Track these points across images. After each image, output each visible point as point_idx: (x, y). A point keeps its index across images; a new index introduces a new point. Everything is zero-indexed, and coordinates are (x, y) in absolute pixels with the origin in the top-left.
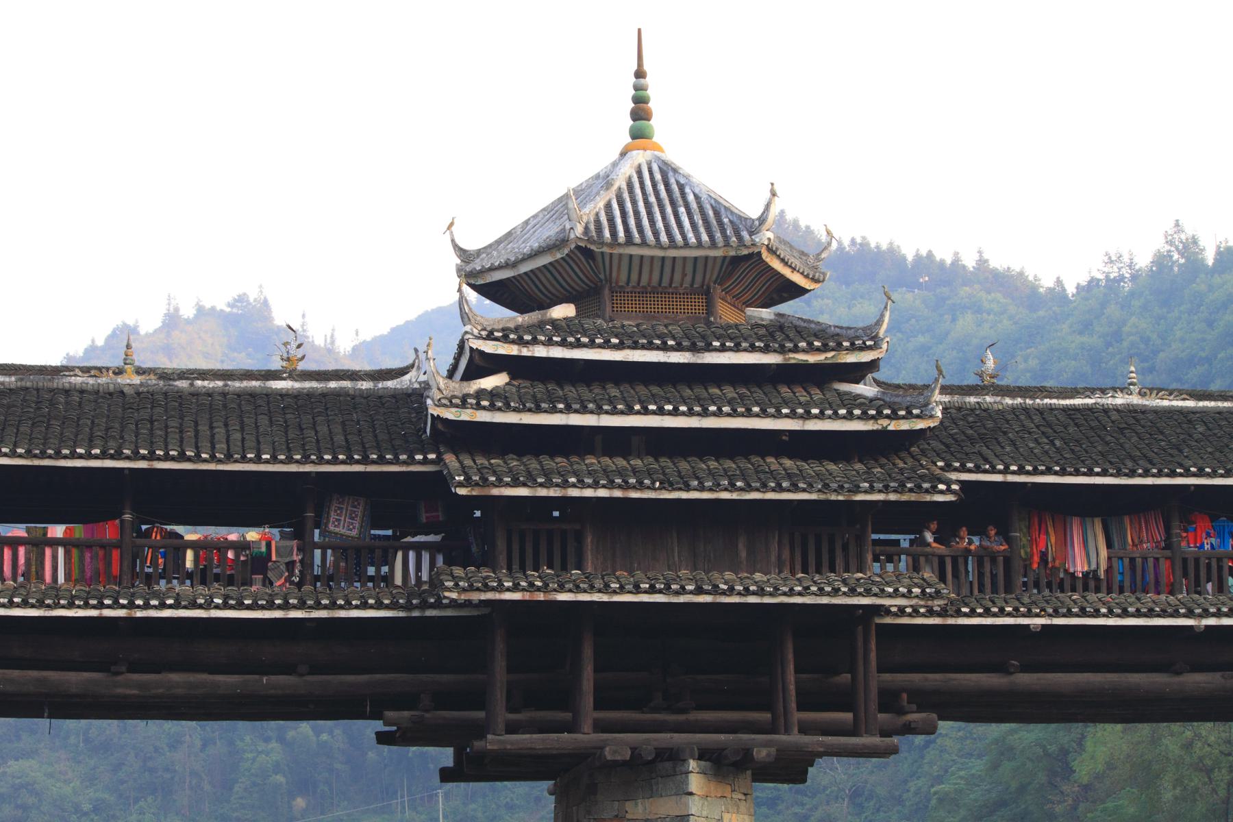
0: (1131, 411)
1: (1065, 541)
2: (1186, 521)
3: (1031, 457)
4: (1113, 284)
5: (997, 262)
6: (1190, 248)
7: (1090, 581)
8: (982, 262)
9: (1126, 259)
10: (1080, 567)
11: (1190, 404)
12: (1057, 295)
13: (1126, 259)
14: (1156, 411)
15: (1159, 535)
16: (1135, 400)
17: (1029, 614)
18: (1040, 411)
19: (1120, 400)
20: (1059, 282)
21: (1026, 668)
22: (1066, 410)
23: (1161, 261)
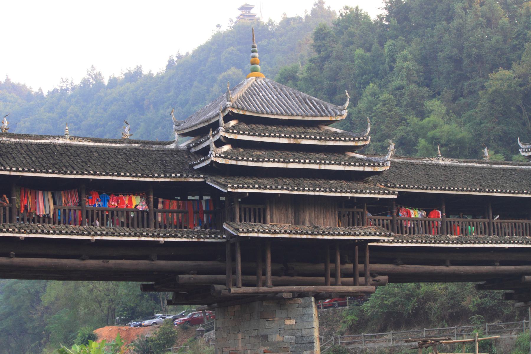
0: (66, 147)
1: (35, 203)
2: (88, 194)
3: (22, 164)
4: (64, 91)
5: (14, 80)
6: (98, 77)
7: (46, 219)
8: (8, 80)
9: (70, 81)
10: (41, 212)
11: (92, 144)
12: (40, 95)
13: (70, 81)
14: (77, 147)
15: (76, 200)
16: (68, 141)
17: (19, 232)
18: (26, 145)
19: (61, 141)
20: (40, 89)
21: (17, 256)
22: (38, 145)
23: (85, 82)
